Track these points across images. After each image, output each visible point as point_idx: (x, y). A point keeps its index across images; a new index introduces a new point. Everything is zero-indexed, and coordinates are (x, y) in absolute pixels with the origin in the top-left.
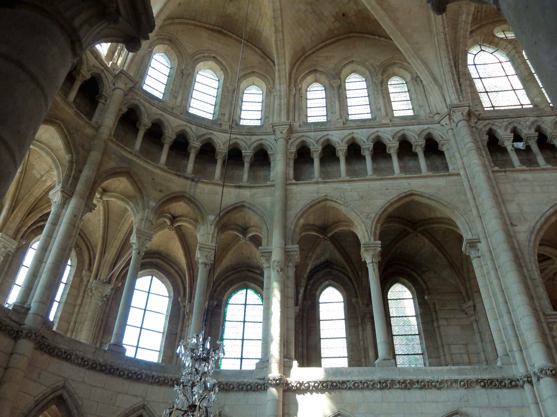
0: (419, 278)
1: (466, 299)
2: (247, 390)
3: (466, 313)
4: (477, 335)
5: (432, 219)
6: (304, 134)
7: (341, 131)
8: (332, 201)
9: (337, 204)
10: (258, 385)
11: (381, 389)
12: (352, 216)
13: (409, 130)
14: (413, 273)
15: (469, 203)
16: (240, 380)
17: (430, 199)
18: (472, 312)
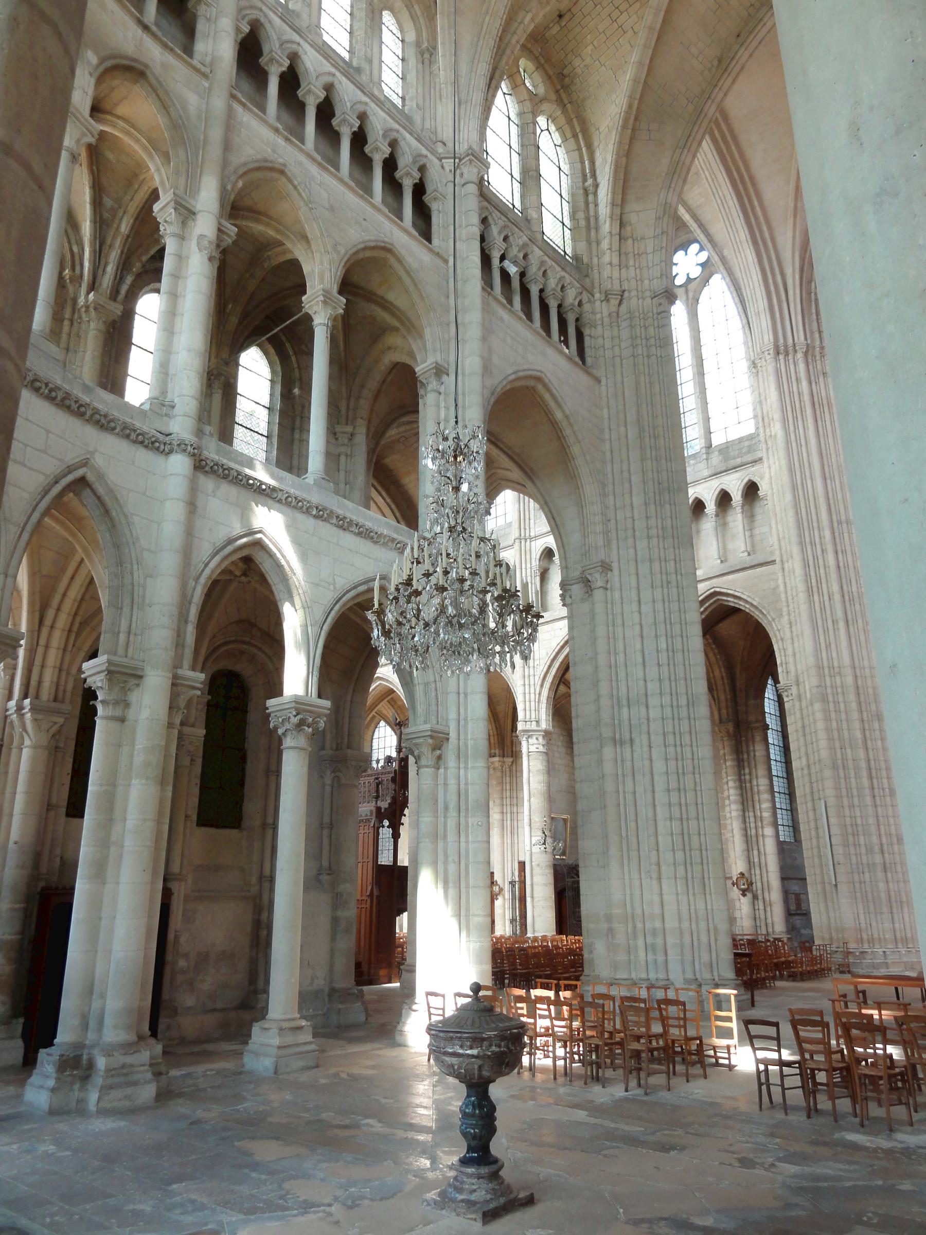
0: (293, 359)
1: (343, 420)
2: (135, 442)
3: (337, 439)
4: (342, 473)
5: (374, 294)
6: (264, 8)
7: (321, 58)
8: (290, 181)
9: (295, 193)
10: (156, 441)
11: (315, 517)
12: (312, 230)
13: (404, 139)
14: (287, 345)
15: (448, 311)
16: (128, 420)
17: (408, 273)
18: (346, 441)
